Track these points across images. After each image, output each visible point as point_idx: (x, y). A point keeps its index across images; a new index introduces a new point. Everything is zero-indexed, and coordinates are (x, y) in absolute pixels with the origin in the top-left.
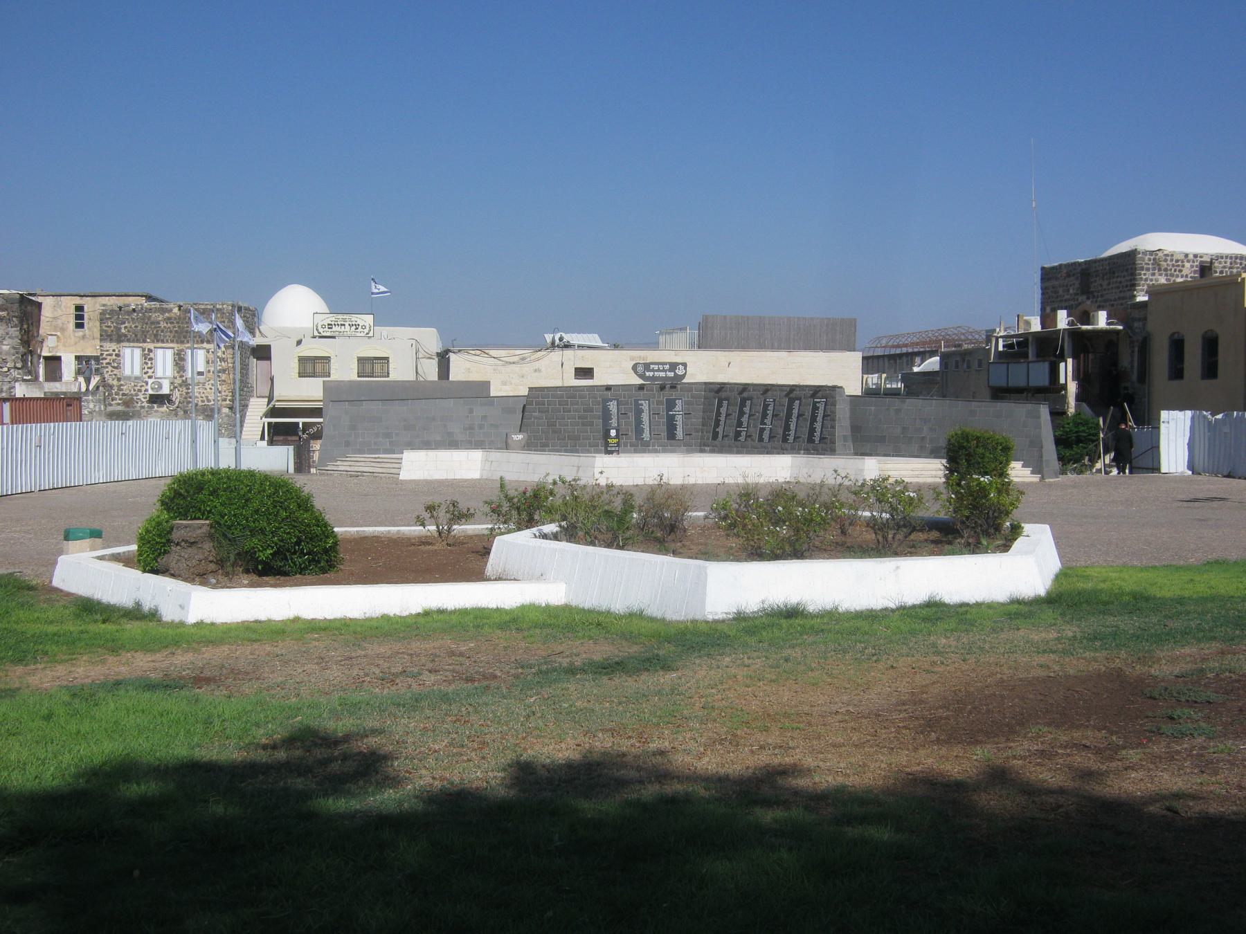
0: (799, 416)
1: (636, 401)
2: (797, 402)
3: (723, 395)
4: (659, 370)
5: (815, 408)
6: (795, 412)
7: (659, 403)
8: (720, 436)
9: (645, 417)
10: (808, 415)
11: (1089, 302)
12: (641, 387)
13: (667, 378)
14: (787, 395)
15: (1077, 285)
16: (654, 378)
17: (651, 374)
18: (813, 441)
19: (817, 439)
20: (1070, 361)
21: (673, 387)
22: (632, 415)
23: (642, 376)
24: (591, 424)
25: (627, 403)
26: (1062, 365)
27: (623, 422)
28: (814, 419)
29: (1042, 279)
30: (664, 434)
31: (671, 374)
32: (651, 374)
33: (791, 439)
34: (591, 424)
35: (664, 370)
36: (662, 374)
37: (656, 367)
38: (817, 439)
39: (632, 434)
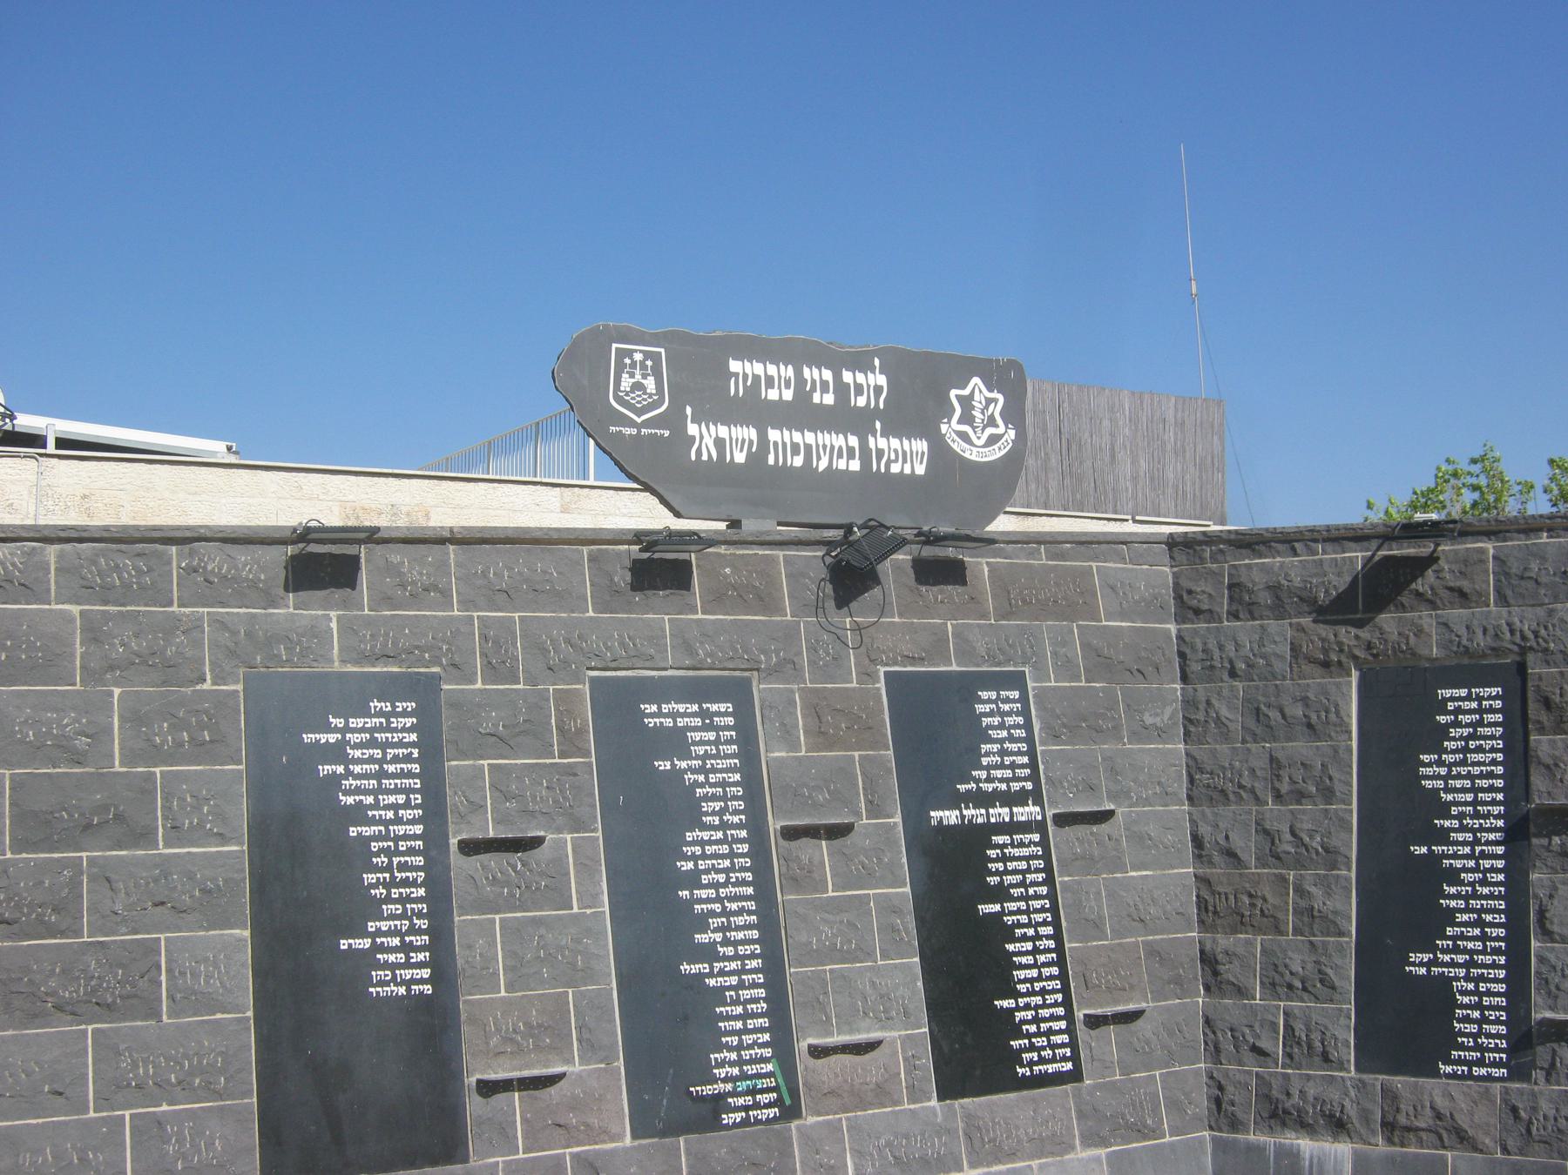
1: (618, 704)
3: (1419, 629)
4: (801, 413)
7: (832, 721)
8: (1480, 1020)
9: (713, 860)
12: (658, 568)
13: (873, 481)
16: (757, 481)
17: (739, 440)
21: (940, 572)
22: (577, 850)
23: (643, 465)
24: (124, 992)
25: (523, 732)
27: (485, 935)
30: (907, 1037)
31: (906, 456)
32: (739, 440)
34: (124, 992)
35: (843, 418)
36: (833, 451)
37: (778, 381)
39: (596, 1073)
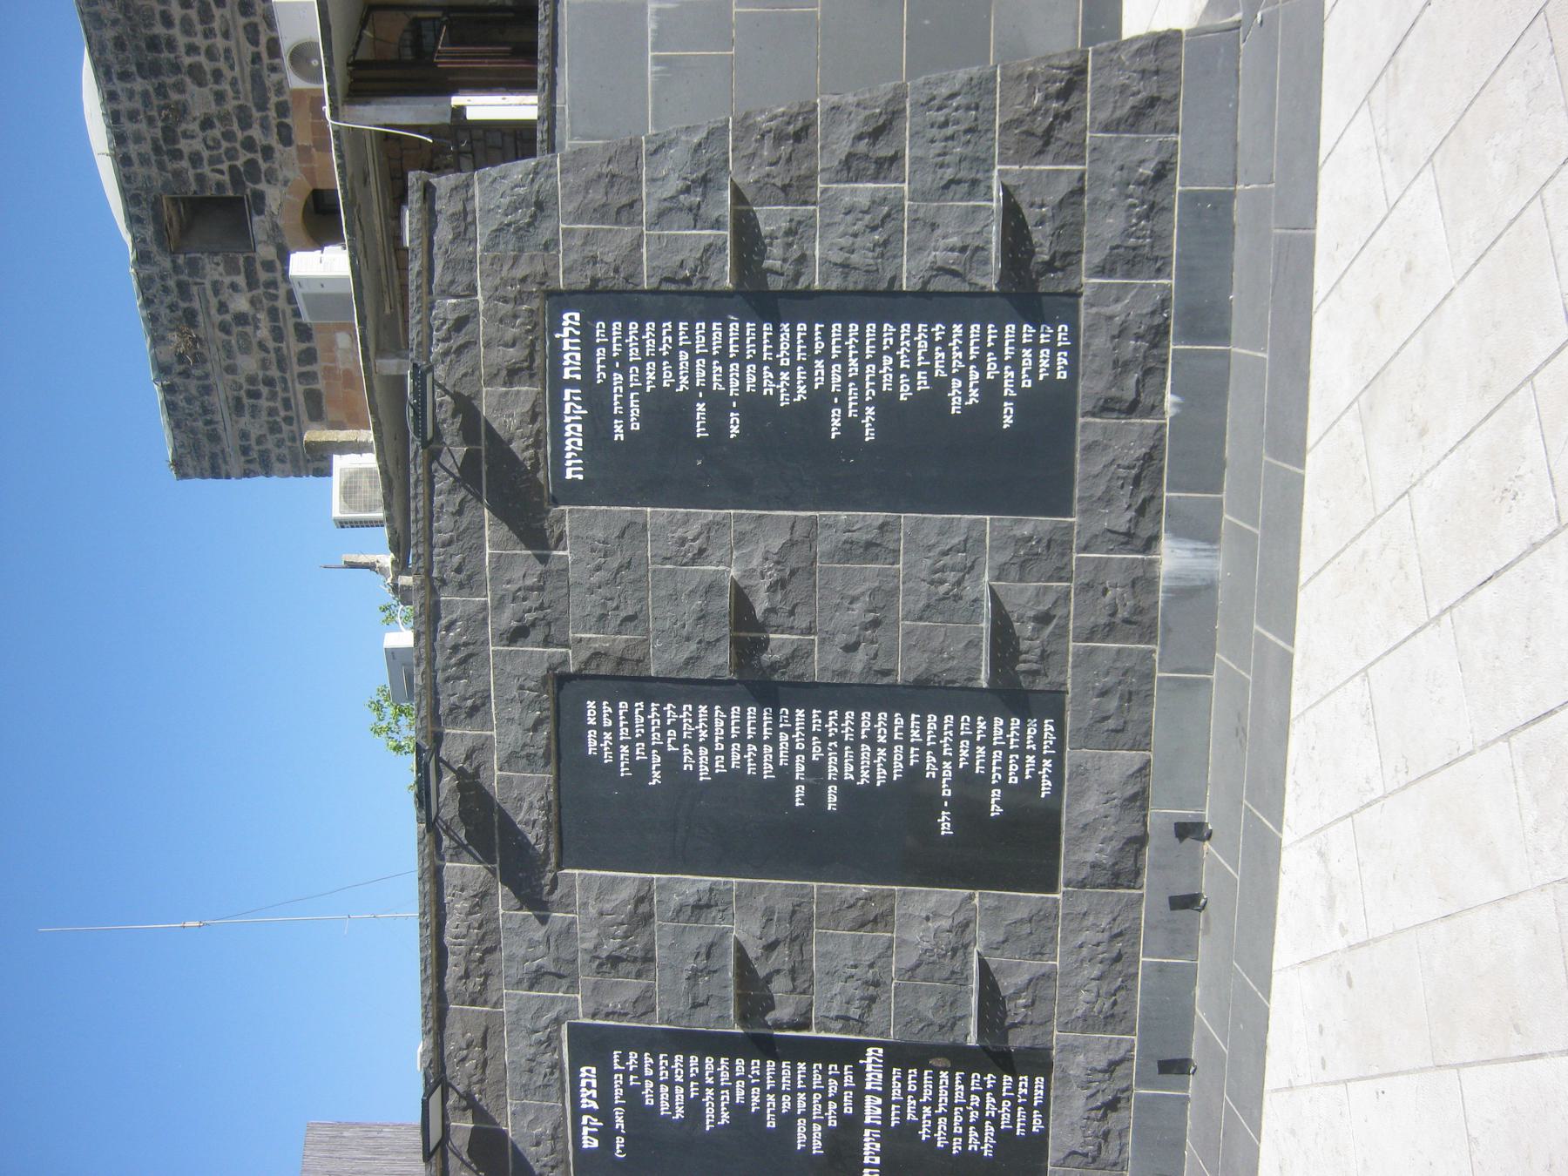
0: (761, 684)
2: (613, 733)
5: (665, 458)
6: (720, 742)
10: (741, 547)
11: (274, 196)
14: (523, 874)
15: (213, 270)
18: (1050, 407)
19: (1027, 358)
20: (456, 100)
26: (472, 115)
28: (785, 457)
29: (215, 473)
33: (1003, 752)
38: (1027, 358)
